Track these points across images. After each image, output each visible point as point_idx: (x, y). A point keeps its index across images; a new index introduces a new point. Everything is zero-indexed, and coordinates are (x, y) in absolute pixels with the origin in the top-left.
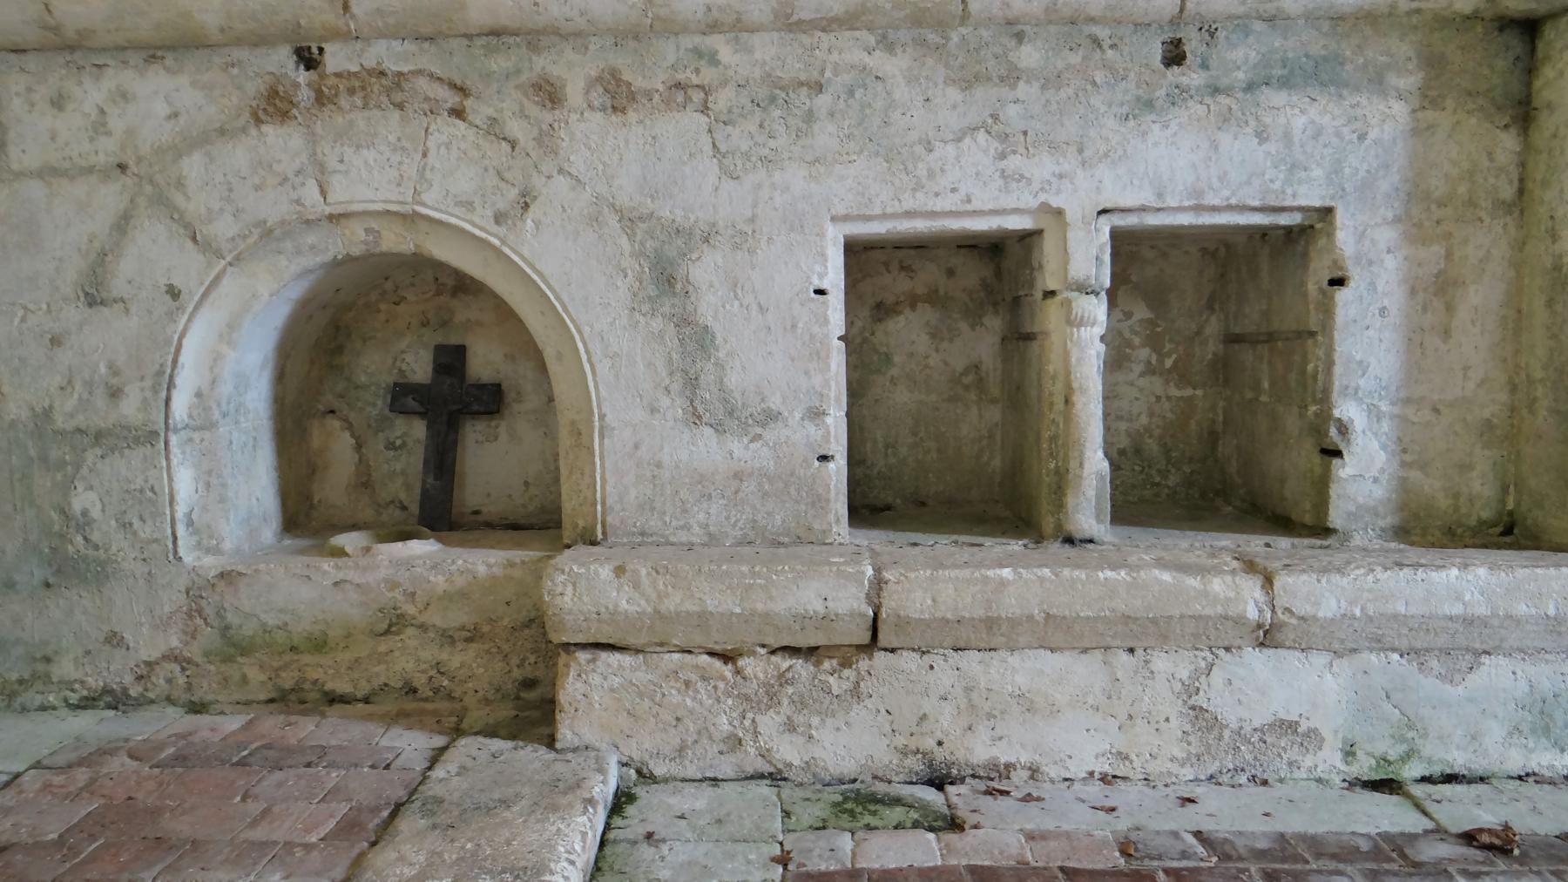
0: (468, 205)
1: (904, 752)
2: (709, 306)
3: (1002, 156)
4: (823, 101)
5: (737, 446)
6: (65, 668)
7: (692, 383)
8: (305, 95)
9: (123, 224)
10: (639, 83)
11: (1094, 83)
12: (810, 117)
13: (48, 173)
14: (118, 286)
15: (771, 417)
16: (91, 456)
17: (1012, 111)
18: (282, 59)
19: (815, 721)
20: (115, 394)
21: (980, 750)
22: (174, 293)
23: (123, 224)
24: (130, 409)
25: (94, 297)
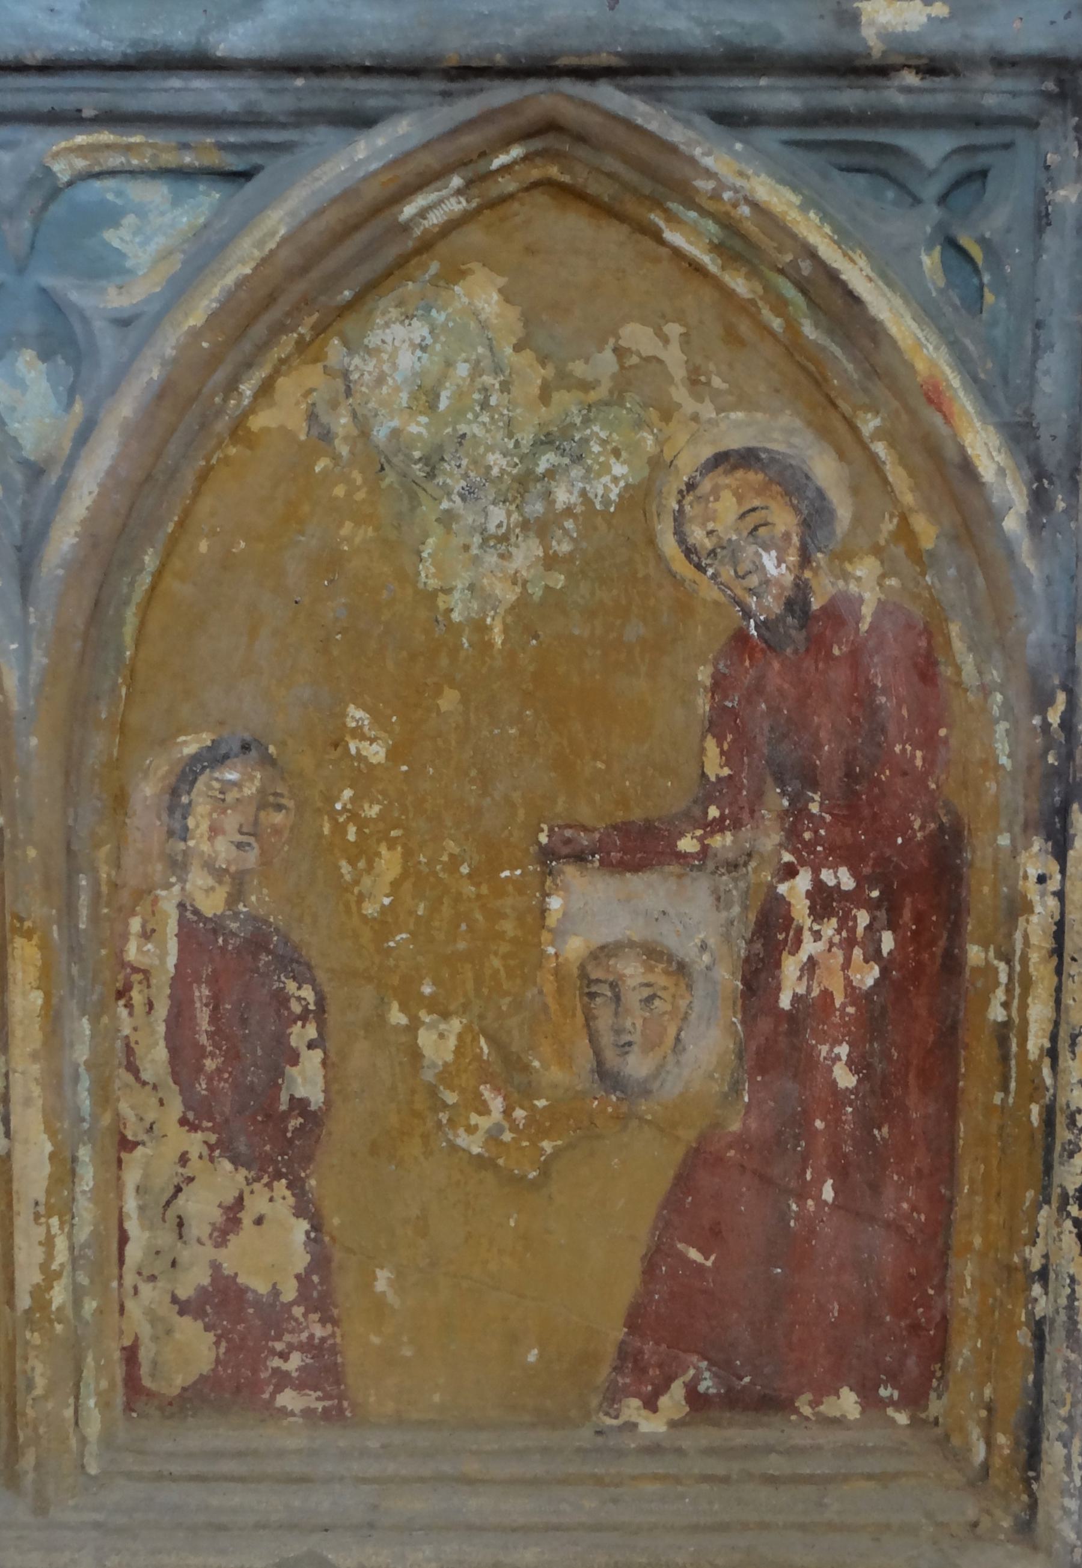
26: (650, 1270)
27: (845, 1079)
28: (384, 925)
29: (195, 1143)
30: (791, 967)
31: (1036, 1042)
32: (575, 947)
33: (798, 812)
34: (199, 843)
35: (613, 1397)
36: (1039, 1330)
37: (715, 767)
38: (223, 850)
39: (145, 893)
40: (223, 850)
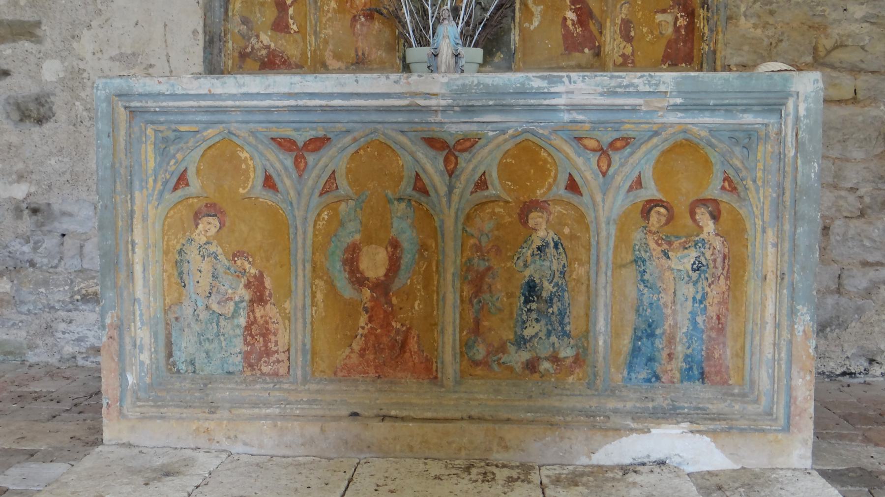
26: (665, 52)
27: (683, 33)
28: (640, 19)
29: (621, 40)
30: (678, 22)
31: (702, 27)
32: (658, 21)
33: (679, 8)
34: (623, 11)
35: (661, 65)
36: (702, 54)
37: (671, 4)
38: (625, 12)
39: (618, 16)
40: (625, 12)
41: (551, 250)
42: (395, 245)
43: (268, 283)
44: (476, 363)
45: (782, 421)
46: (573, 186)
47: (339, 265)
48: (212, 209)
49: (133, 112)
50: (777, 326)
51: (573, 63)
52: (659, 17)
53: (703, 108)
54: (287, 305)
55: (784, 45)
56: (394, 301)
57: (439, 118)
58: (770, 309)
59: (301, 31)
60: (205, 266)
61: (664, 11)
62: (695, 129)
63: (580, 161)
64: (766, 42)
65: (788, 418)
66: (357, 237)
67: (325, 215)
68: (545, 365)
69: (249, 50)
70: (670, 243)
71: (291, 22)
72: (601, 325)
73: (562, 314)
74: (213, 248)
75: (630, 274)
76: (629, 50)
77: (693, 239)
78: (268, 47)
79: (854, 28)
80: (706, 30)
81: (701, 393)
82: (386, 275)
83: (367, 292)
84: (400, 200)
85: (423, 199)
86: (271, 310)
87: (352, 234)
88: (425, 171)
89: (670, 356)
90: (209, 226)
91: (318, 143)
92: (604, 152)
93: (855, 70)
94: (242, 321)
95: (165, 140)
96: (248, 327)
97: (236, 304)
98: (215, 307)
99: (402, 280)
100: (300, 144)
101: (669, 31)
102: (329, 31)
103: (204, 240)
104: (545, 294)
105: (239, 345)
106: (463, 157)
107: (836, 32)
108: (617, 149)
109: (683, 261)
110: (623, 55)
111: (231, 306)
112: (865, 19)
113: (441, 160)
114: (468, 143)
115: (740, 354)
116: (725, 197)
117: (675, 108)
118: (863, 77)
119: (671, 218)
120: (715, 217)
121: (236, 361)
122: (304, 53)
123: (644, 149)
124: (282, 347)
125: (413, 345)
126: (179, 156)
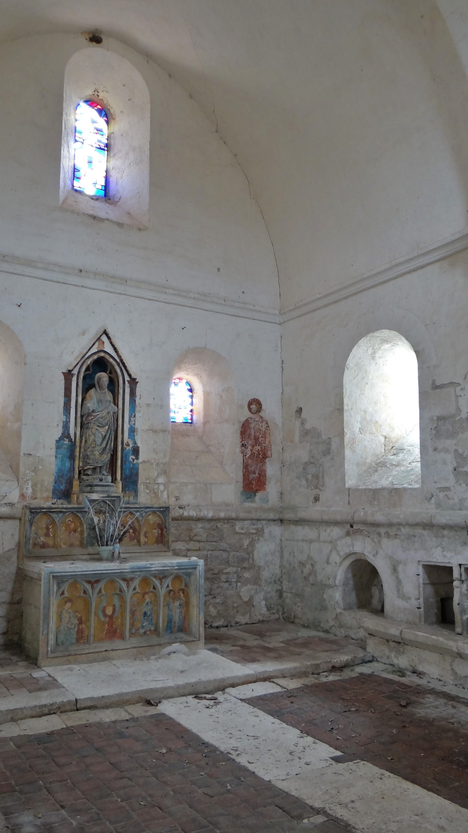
0: (370, 553)
1: (411, 666)
2: (401, 576)
3: (442, 552)
4: (416, 539)
5: (405, 603)
6: (322, 625)
7: (398, 590)
8: (351, 532)
9: (331, 551)
10: (391, 534)
11: (456, 539)
12: (414, 542)
13: (324, 542)
14: (330, 562)
15: (410, 598)
16: (327, 588)
17: (444, 543)
18: (348, 526)
19: (398, 656)
20: (329, 579)
21: (420, 668)
22: (336, 563)
23: (331, 551)
24: (331, 582)
25: (328, 563)
41: (149, 604)
42: (114, 606)
43: (83, 618)
44: (132, 634)
45: (198, 639)
46: (154, 588)
47: (101, 612)
48: (69, 600)
49: (53, 576)
50: (197, 617)
51: (132, 544)
52: (154, 531)
53: (181, 569)
54: (88, 624)
55: (182, 535)
56: (114, 620)
57: (126, 574)
58: (195, 613)
59: (54, 536)
60: (67, 616)
61: (155, 529)
62: (179, 573)
63: (156, 582)
64: (178, 534)
65: (199, 638)
66: (105, 604)
67: (98, 600)
68: (148, 632)
69: (37, 542)
70: (174, 600)
71: (51, 533)
72: (161, 621)
73: (152, 619)
74: (70, 611)
75: (166, 608)
76: (146, 540)
77: (179, 599)
78: (43, 541)
79: (199, 530)
80: (166, 535)
81: (182, 635)
82: (112, 613)
83: (107, 619)
84: (116, 594)
85: (122, 594)
86: (83, 626)
87: (104, 604)
88: (122, 587)
89: (175, 627)
90: (69, 605)
91: (97, 581)
92: (161, 580)
93: (199, 541)
94: (76, 629)
95: (58, 583)
96: (77, 631)
97: (75, 625)
98: (69, 626)
99: (116, 614)
100: (93, 582)
101: (156, 535)
102: (62, 536)
103: (67, 608)
104: (148, 615)
105: (75, 636)
106: (131, 583)
107: (195, 531)
108: (163, 579)
109: (177, 604)
110: (145, 542)
111: (73, 626)
112: (201, 528)
113: (126, 584)
114: (132, 579)
115: (189, 624)
116: (185, 588)
117: (176, 569)
118: (201, 543)
119: (174, 593)
120: (183, 593)
121: (74, 641)
122: (54, 543)
123: (170, 578)
124: (86, 635)
125: (118, 631)
126: (63, 587)
